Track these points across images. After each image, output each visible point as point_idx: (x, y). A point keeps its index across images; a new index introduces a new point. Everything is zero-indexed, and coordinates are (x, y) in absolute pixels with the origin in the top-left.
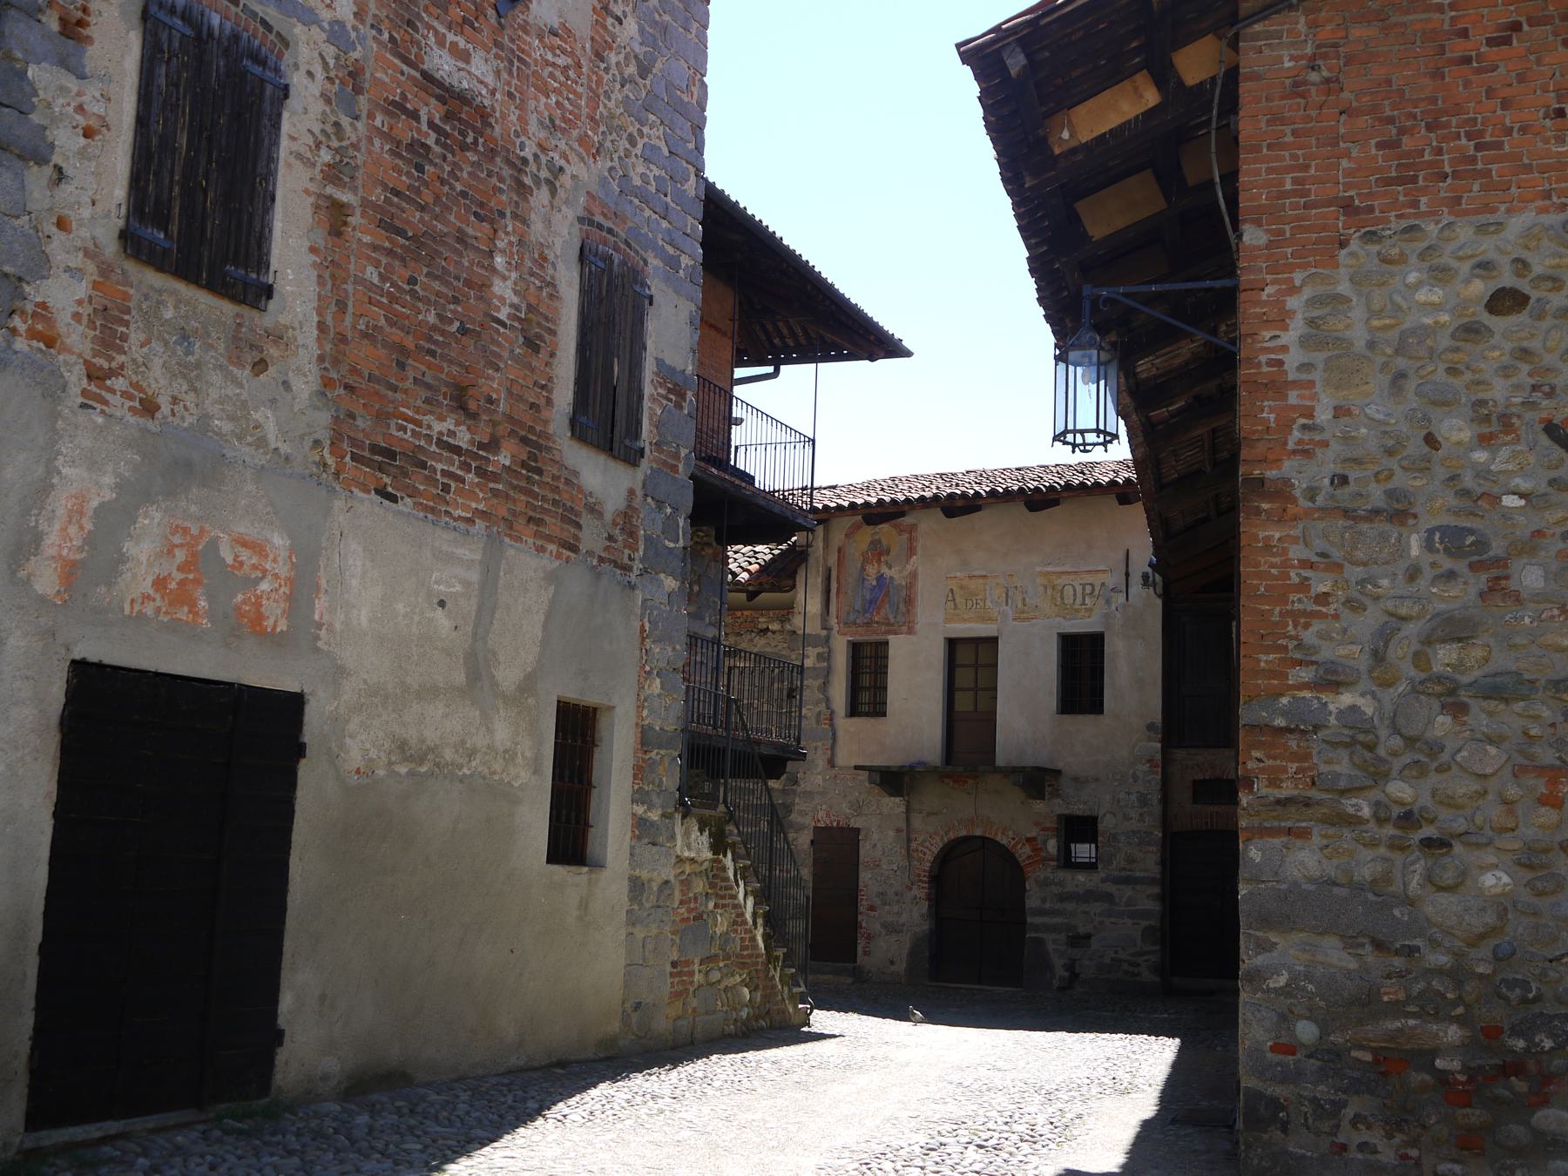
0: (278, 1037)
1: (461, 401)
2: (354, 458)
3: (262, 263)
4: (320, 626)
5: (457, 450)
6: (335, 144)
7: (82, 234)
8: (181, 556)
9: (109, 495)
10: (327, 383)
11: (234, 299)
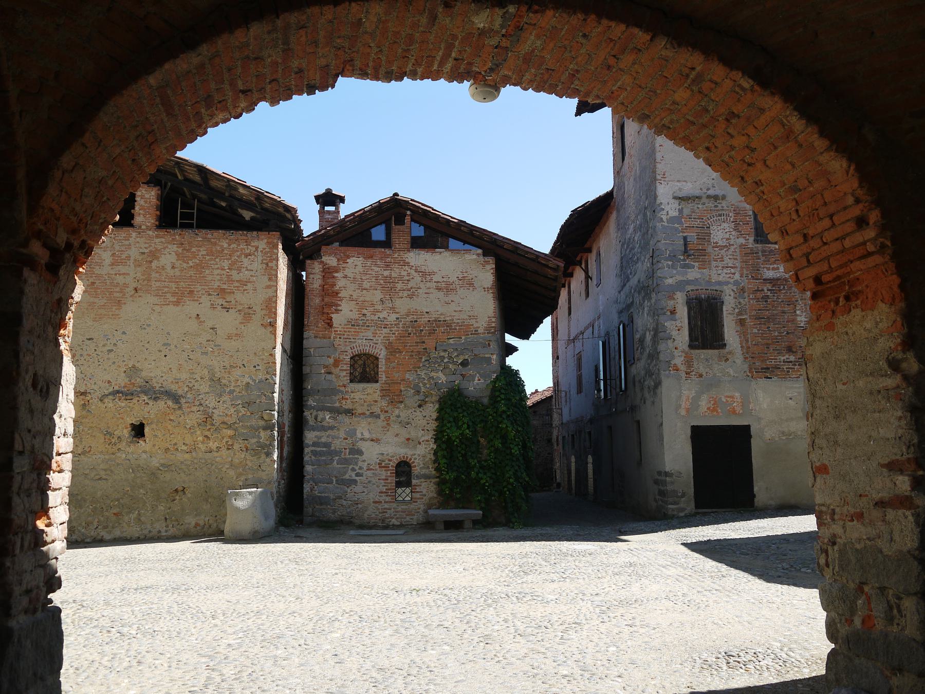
0: (754, 496)
1: (790, 350)
2: (756, 372)
3: (723, 339)
4: (752, 410)
5: (791, 362)
6: (739, 307)
7: (680, 349)
8: (712, 402)
9: (694, 395)
10: (746, 358)
11: (717, 349)
